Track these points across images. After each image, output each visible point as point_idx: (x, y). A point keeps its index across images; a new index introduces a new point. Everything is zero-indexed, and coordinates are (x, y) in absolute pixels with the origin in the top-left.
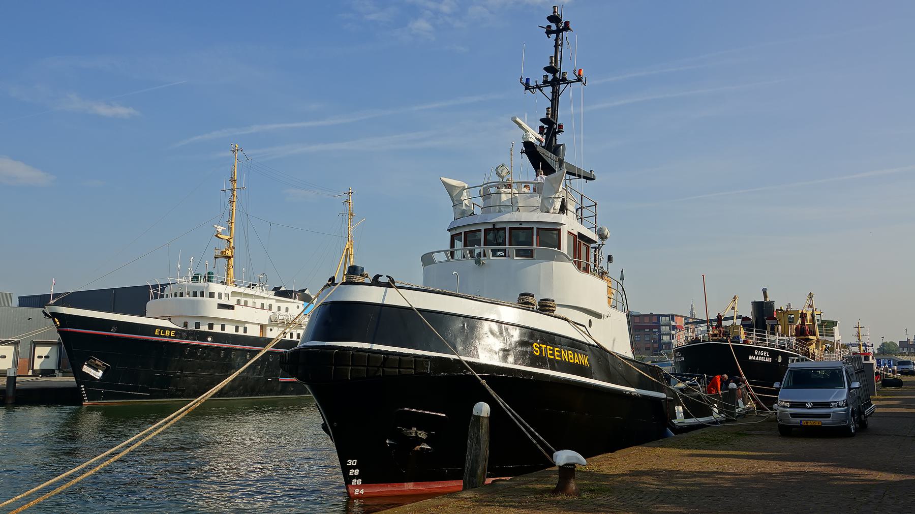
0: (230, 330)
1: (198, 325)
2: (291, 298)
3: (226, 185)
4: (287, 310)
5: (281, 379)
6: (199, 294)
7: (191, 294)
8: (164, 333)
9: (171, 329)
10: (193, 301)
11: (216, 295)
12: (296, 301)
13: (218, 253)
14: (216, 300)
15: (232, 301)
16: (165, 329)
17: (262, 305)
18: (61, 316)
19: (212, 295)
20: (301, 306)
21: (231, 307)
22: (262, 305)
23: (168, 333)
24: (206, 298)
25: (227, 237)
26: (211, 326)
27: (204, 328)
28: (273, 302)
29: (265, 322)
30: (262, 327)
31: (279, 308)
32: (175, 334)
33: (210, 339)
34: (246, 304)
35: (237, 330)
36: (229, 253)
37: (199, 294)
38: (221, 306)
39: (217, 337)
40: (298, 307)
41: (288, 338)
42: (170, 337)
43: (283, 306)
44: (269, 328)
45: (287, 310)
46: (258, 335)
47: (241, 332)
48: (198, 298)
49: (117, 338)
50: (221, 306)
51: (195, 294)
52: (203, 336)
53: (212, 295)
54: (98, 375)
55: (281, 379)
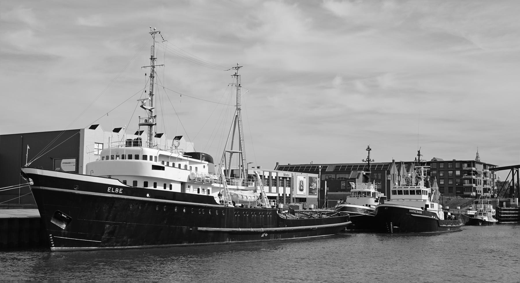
0: (160, 188)
1: (135, 183)
2: (199, 159)
3: (149, 62)
4: (196, 168)
5: (199, 228)
6: (133, 157)
7: (127, 157)
8: (114, 190)
9: (119, 187)
10: (135, 163)
11: (148, 158)
12: (203, 162)
13: (143, 122)
14: (149, 163)
15: (159, 164)
16: (115, 187)
17: (180, 165)
18: (35, 177)
19: (145, 157)
20: (206, 165)
21: (162, 168)
22: (180, 165)
23: (117, 190)
24: (141, 161)
25: (150, 108)
26: (146, 184)
27: (140, 185)
28: (187, 163)
29: (185, 180)
30: (183, 184)
31: (191, 167)
32: (122, 191)
33: (148, 195)
34: (174, 165)
35: (165, 188)
36: (151, 120)
37: (133, 157)
38: (155, 167)
39: (155, 194)
40: (204, 167)
41: (201, 193)
42: (118, 194)
43: (194, 166)
44: (187, 185)
45: (196, 168)
46: (180, 191)
47: (168, 189)
48: (133, 160)
49: (79, 194)
50: (155, 167)
51: (130, 157)
52: (142, 192)
53: (145, 157)
54: (63, 226)
55: (199, 228)
